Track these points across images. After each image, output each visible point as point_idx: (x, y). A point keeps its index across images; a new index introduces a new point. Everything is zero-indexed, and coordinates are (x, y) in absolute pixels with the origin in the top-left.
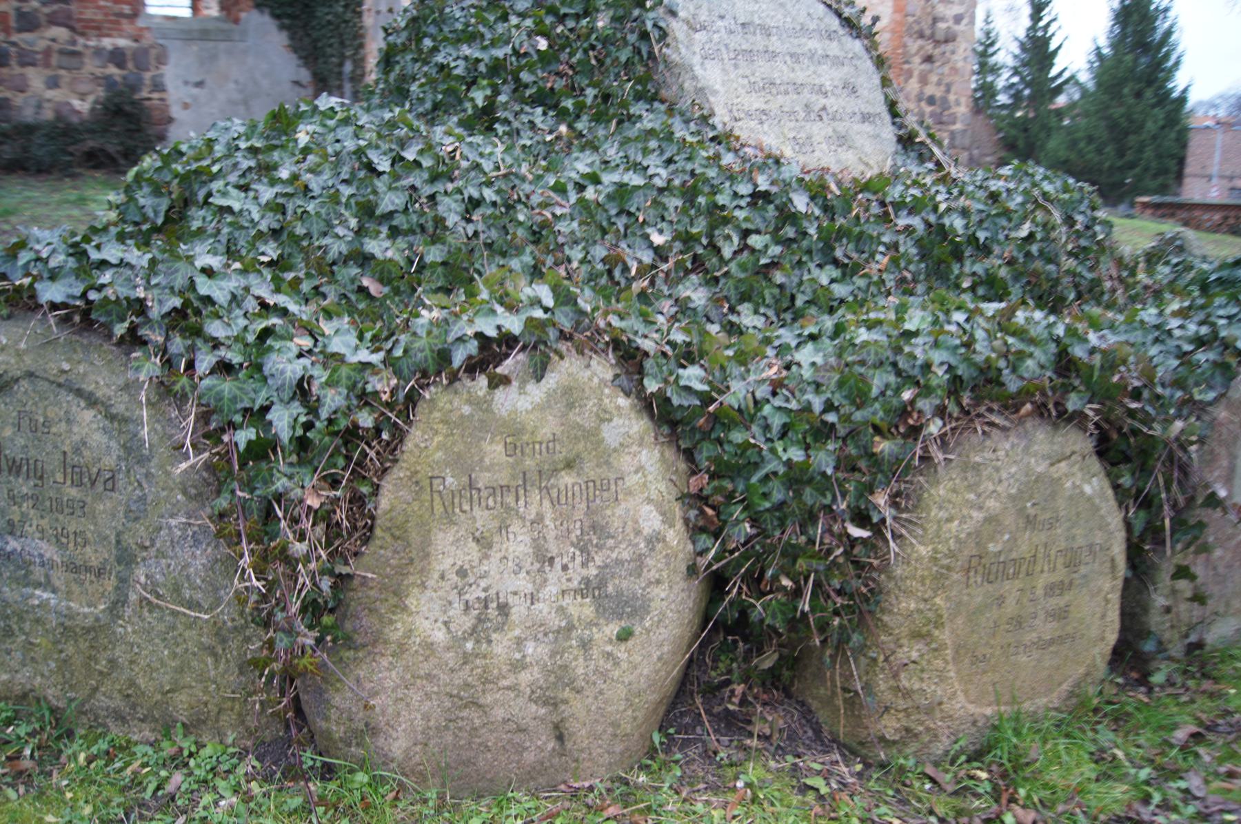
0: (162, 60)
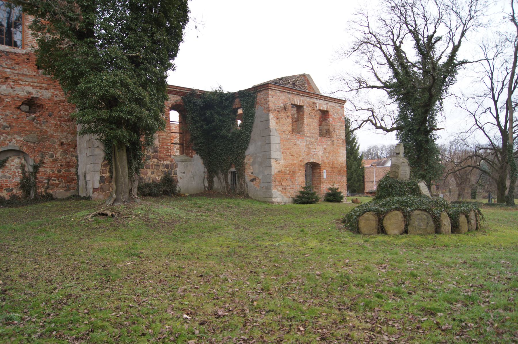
0: (176, 167)
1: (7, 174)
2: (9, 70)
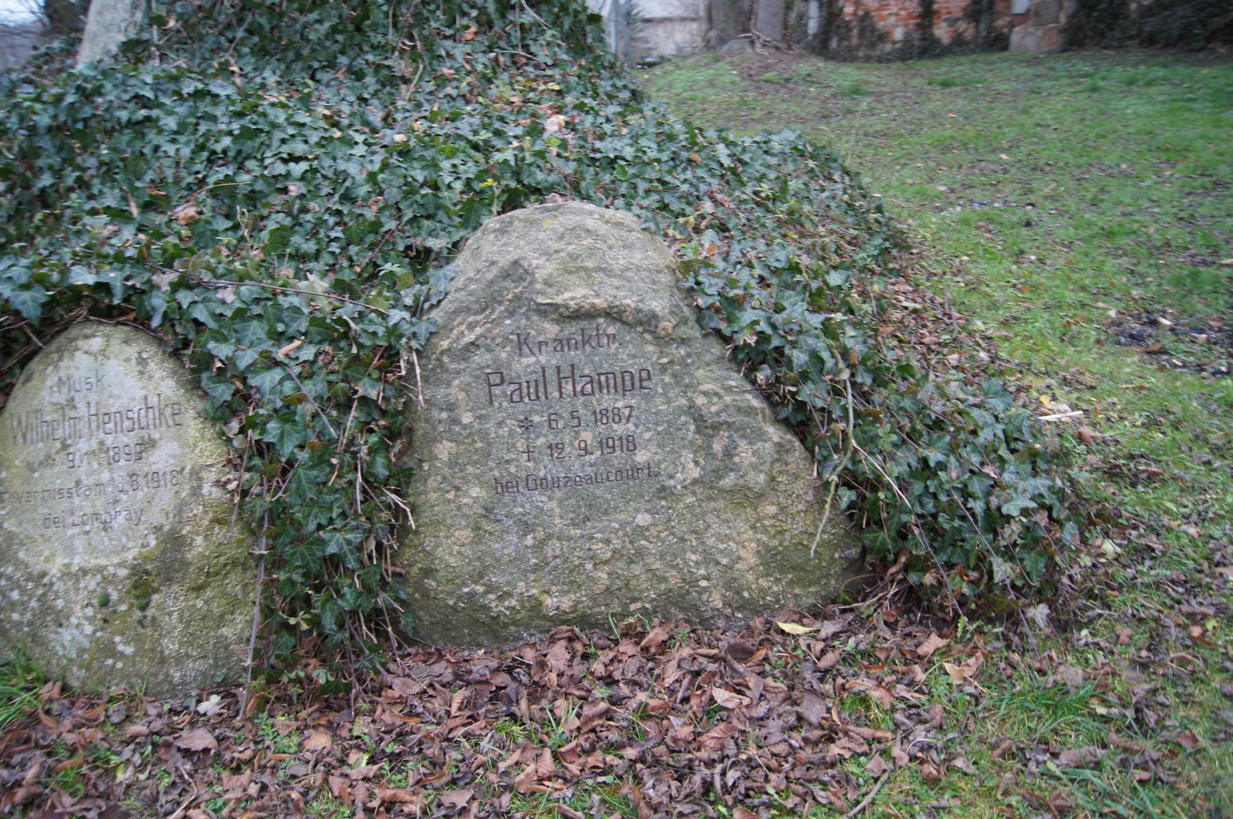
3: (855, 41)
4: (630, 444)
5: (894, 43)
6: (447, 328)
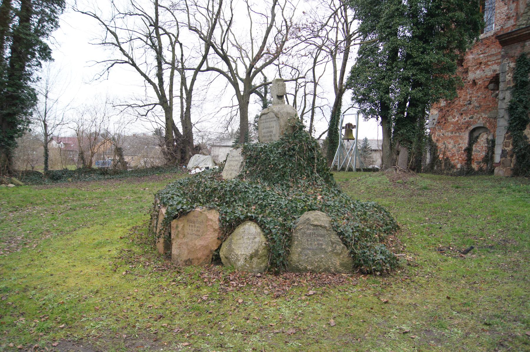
1: (478, 149)
2: (482, 56)
3: (443, 167)
4: (322, 245)
5: (457, 169)
6: (298, 226)
